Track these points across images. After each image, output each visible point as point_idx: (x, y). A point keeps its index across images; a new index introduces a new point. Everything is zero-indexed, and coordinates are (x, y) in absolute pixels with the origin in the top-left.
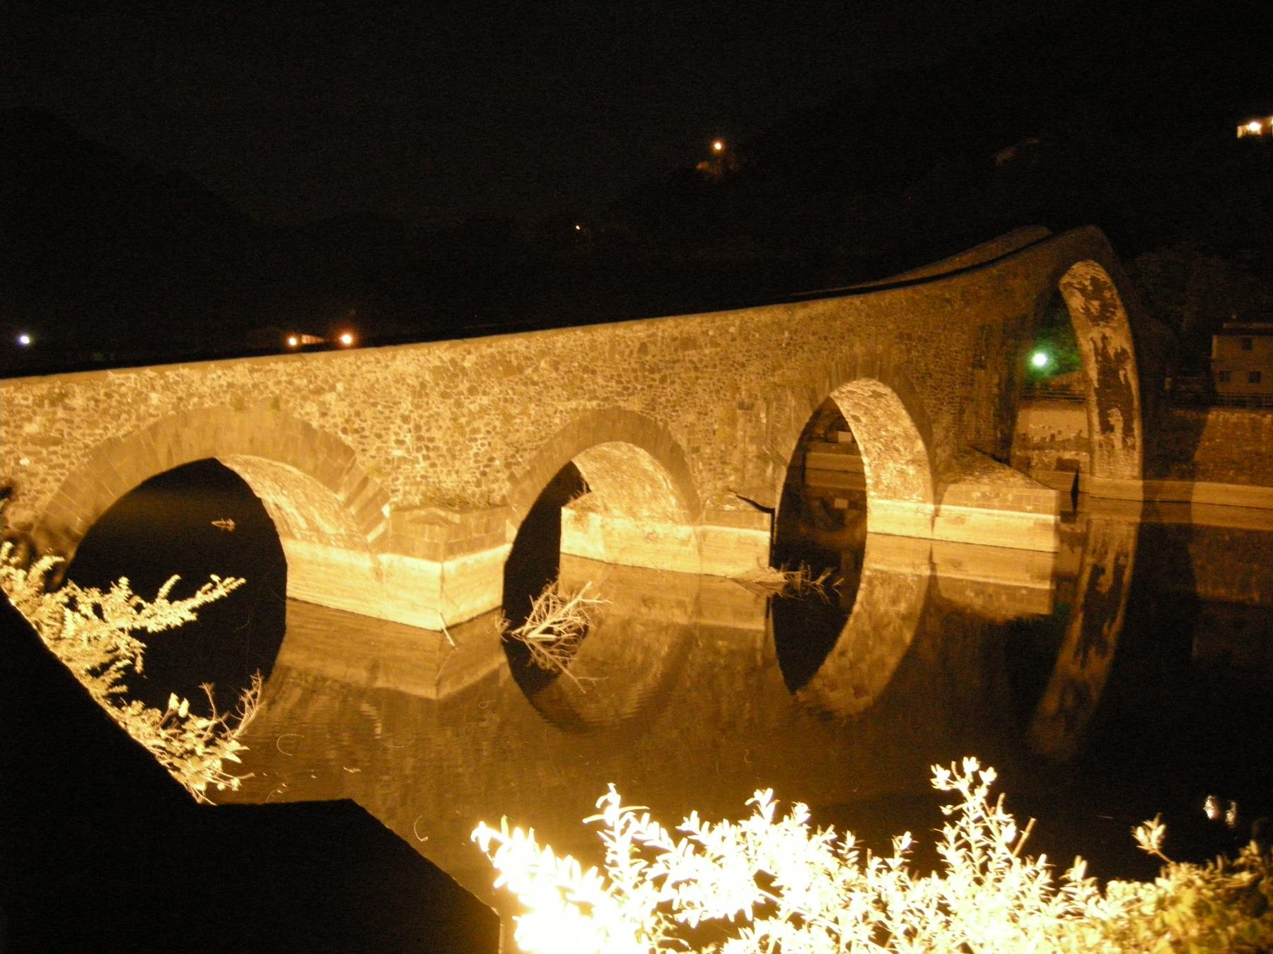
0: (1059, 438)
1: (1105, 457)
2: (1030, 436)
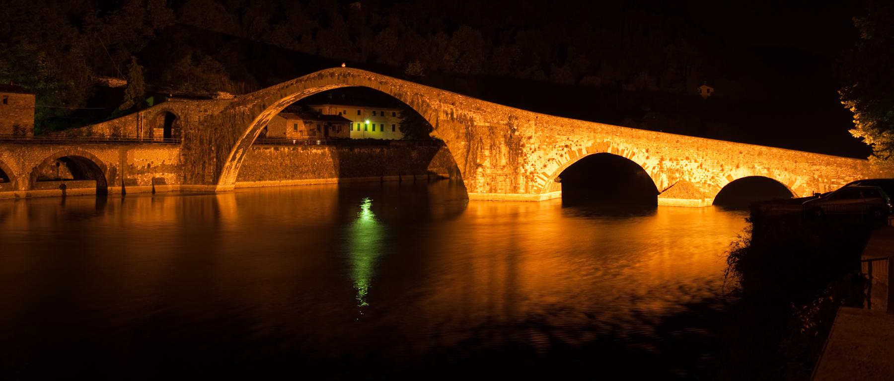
1: (227, 174)
2: (135, 166)
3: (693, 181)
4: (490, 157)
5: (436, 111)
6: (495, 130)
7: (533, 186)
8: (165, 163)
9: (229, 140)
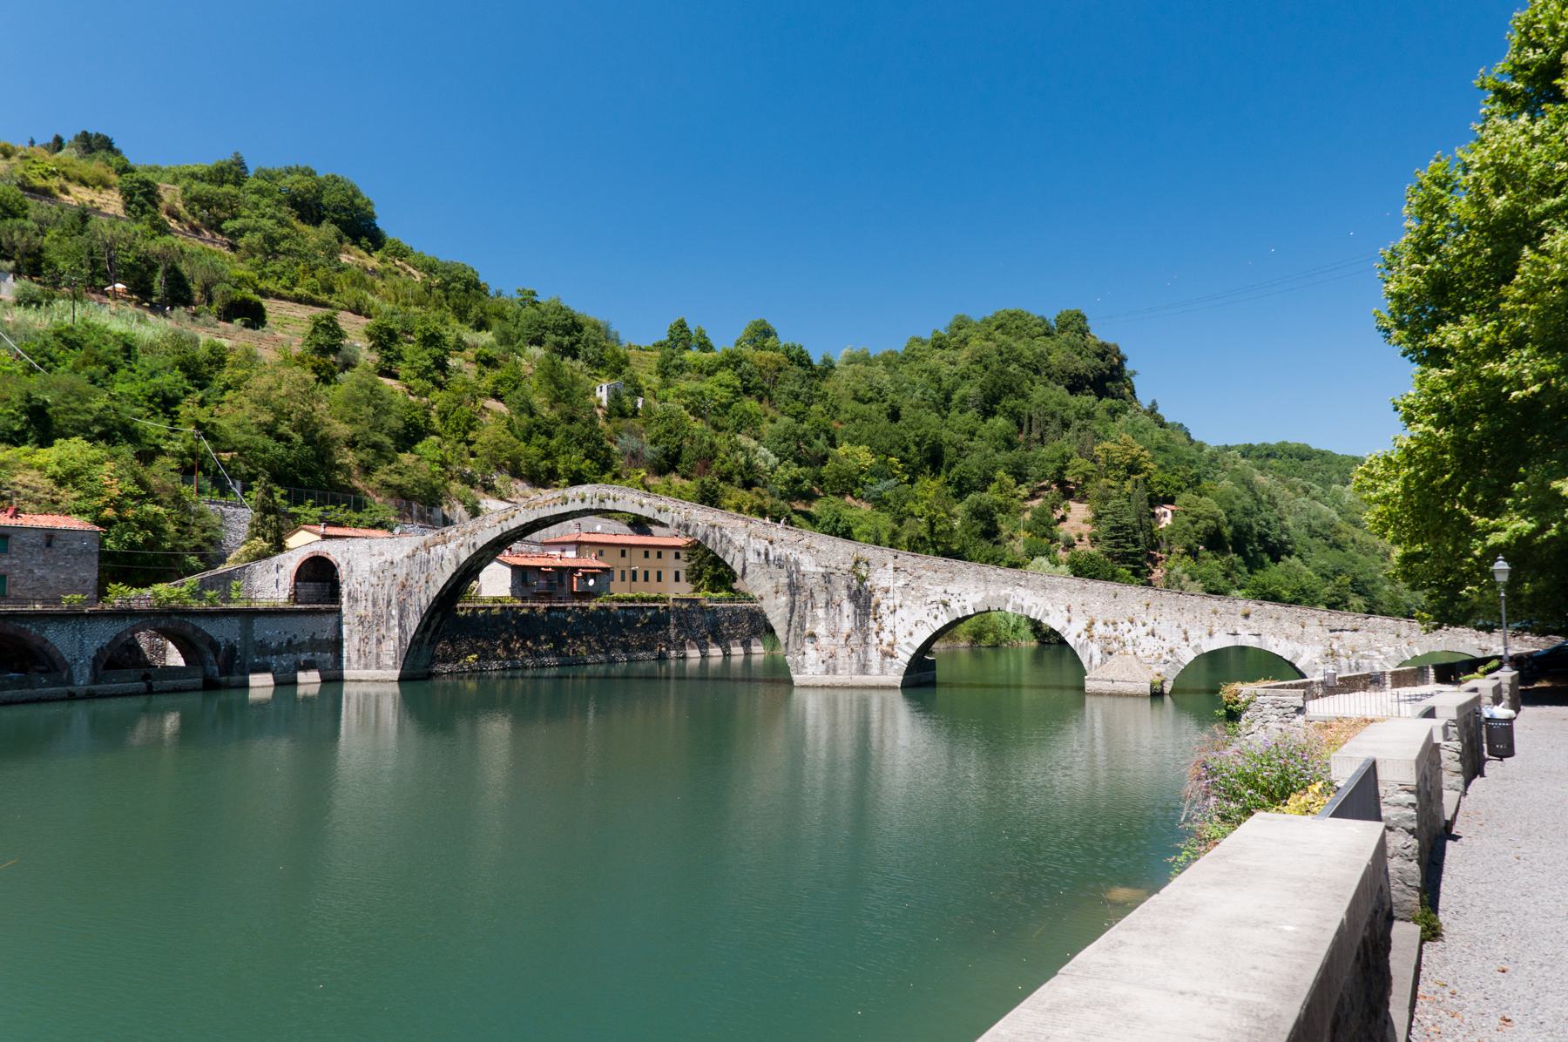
0: (295, 642)
3: (1140, 654)
4: (826, 619)
5: (742, 549)
6: (832, 577)
7: (892, 664)
8: (316, 636)
9: (420, 599)
